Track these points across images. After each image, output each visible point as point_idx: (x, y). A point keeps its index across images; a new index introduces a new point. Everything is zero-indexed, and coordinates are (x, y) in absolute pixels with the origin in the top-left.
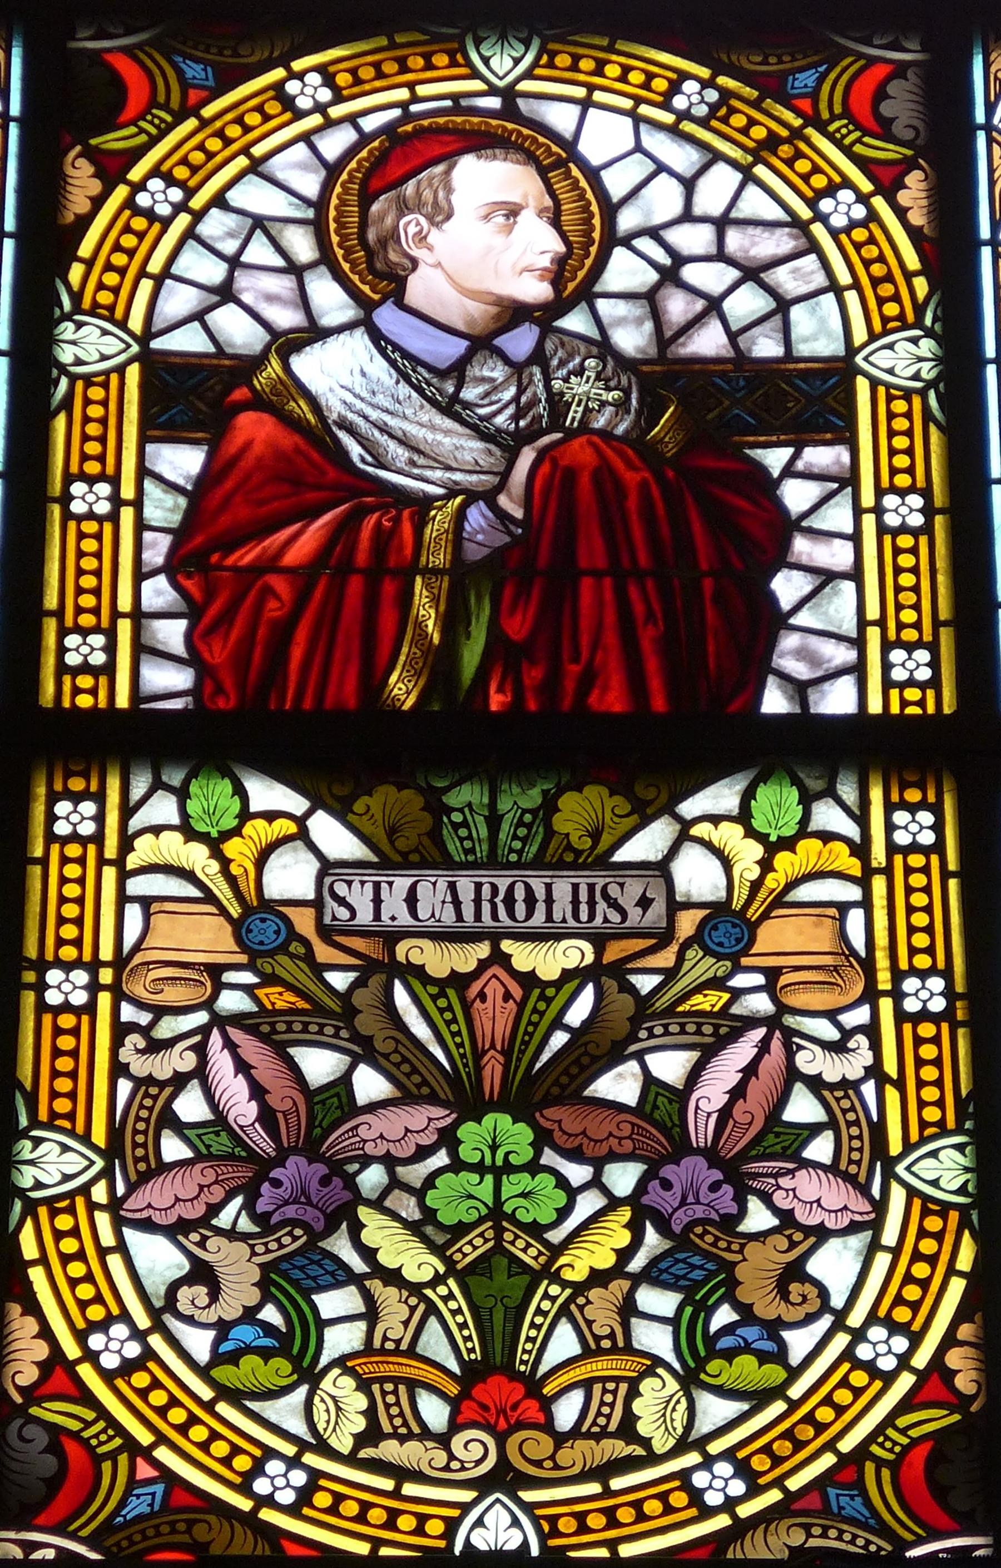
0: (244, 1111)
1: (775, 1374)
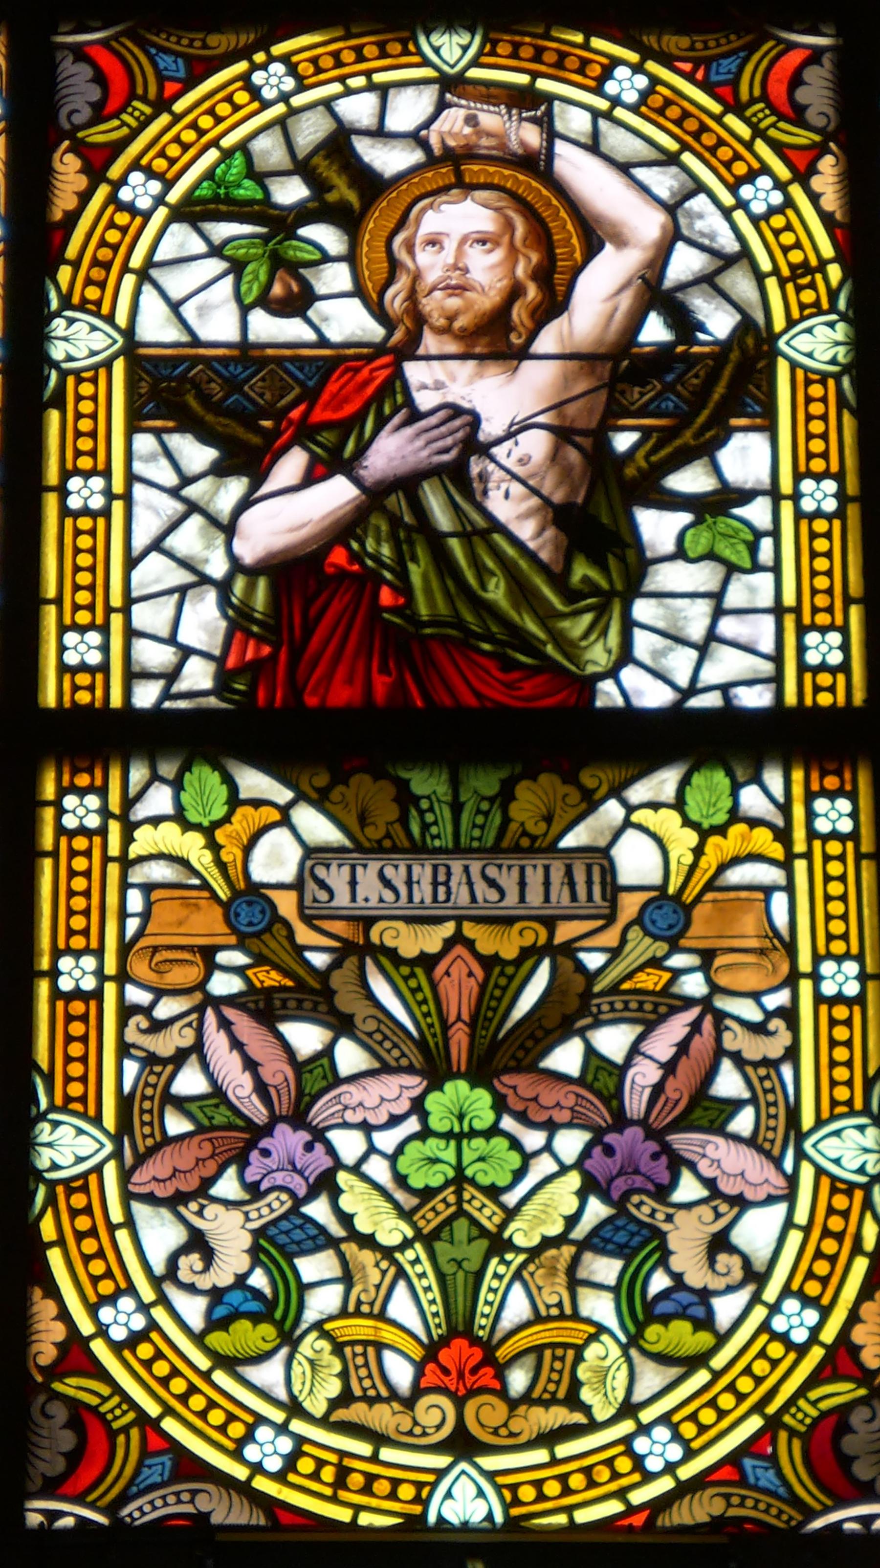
0: (239, 1085)
1: (705, 1339)
